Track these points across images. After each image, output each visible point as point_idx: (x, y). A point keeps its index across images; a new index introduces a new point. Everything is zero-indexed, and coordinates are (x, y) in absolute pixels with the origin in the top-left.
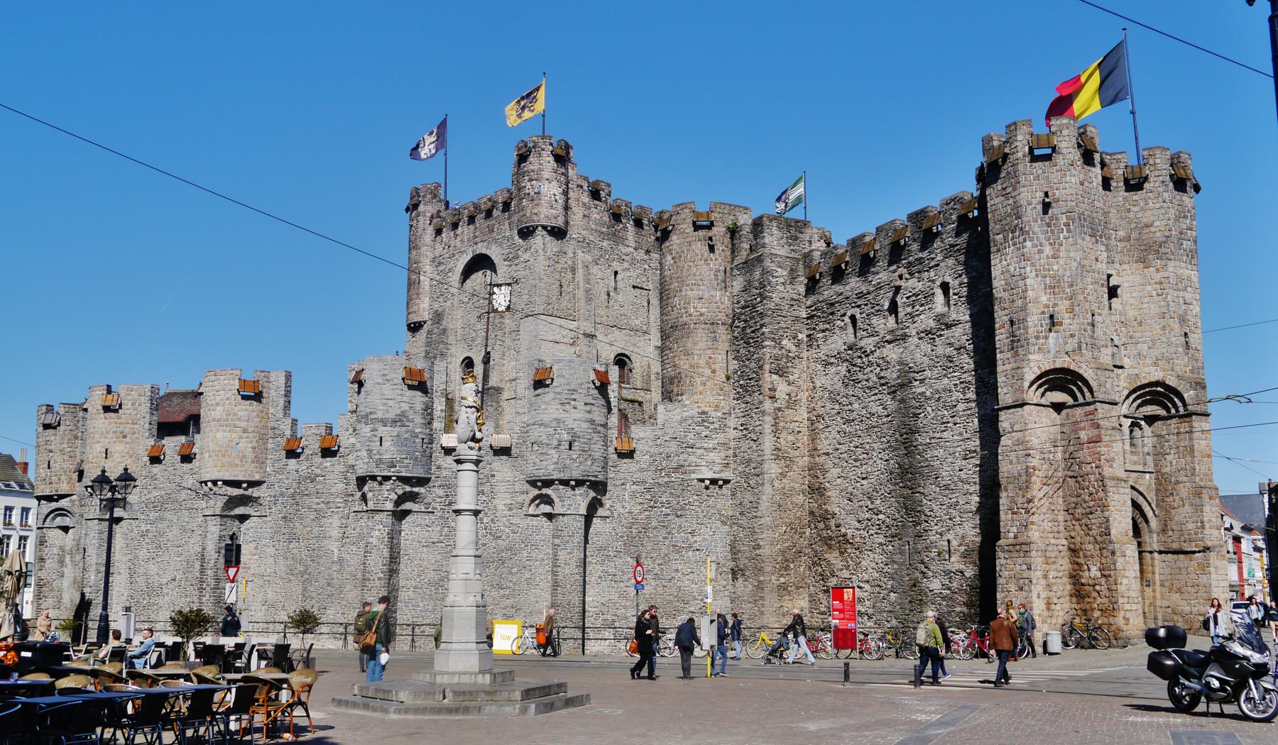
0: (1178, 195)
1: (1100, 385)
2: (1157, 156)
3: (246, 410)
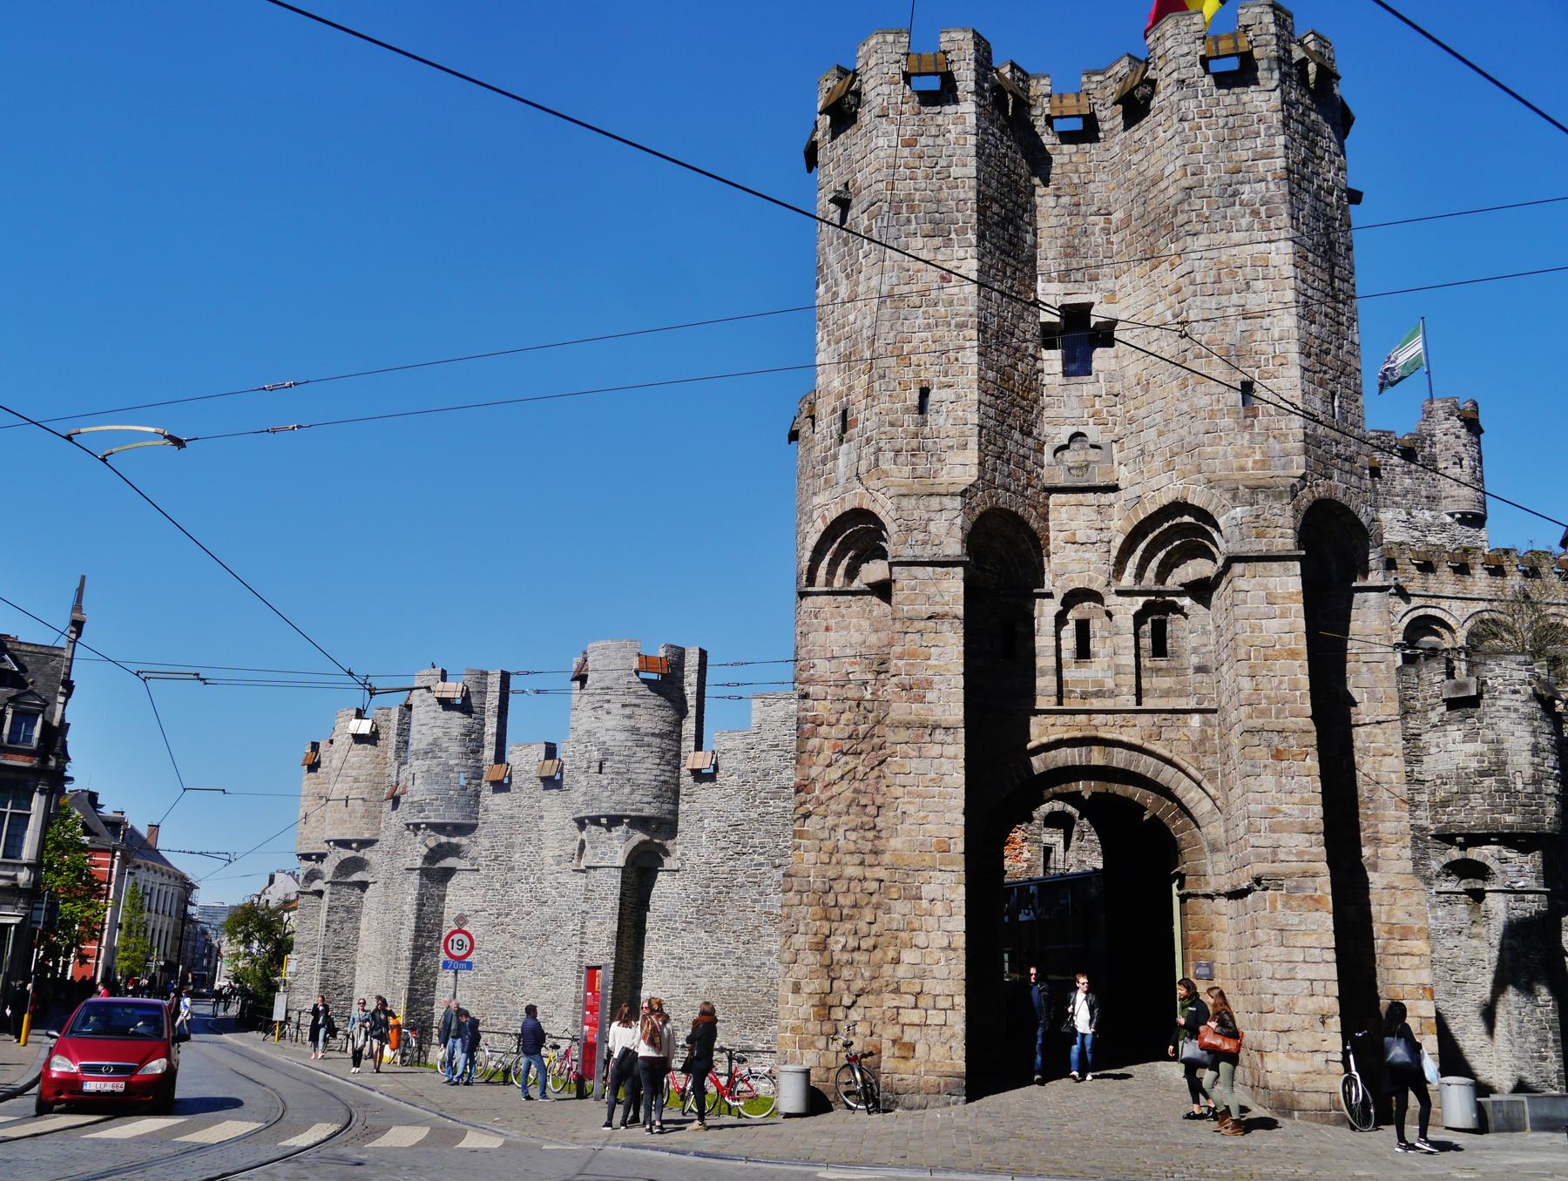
0: (1228, 97)
2: (1168, 34)
3: (358, 755)
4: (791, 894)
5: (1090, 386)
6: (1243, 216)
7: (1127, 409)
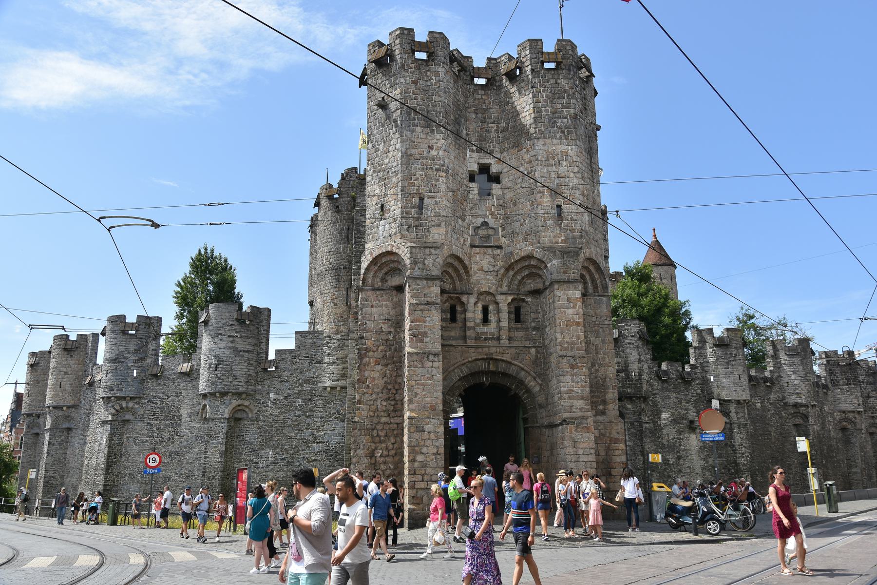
4: (356, 431)
5: (490, 201)
6: (558, 133)
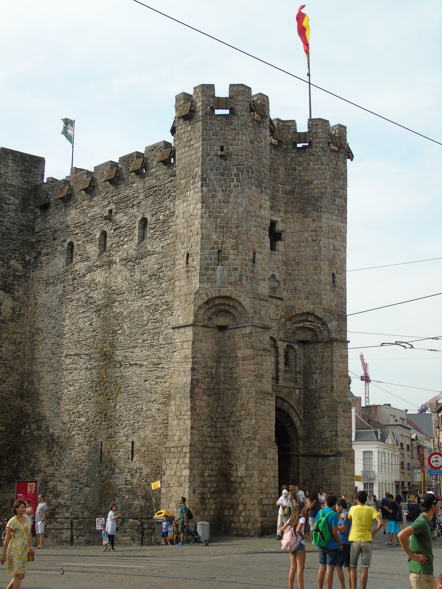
1: (255, 312)
2: (320, 126)
4: (192, 453)
7: (288, 269)
